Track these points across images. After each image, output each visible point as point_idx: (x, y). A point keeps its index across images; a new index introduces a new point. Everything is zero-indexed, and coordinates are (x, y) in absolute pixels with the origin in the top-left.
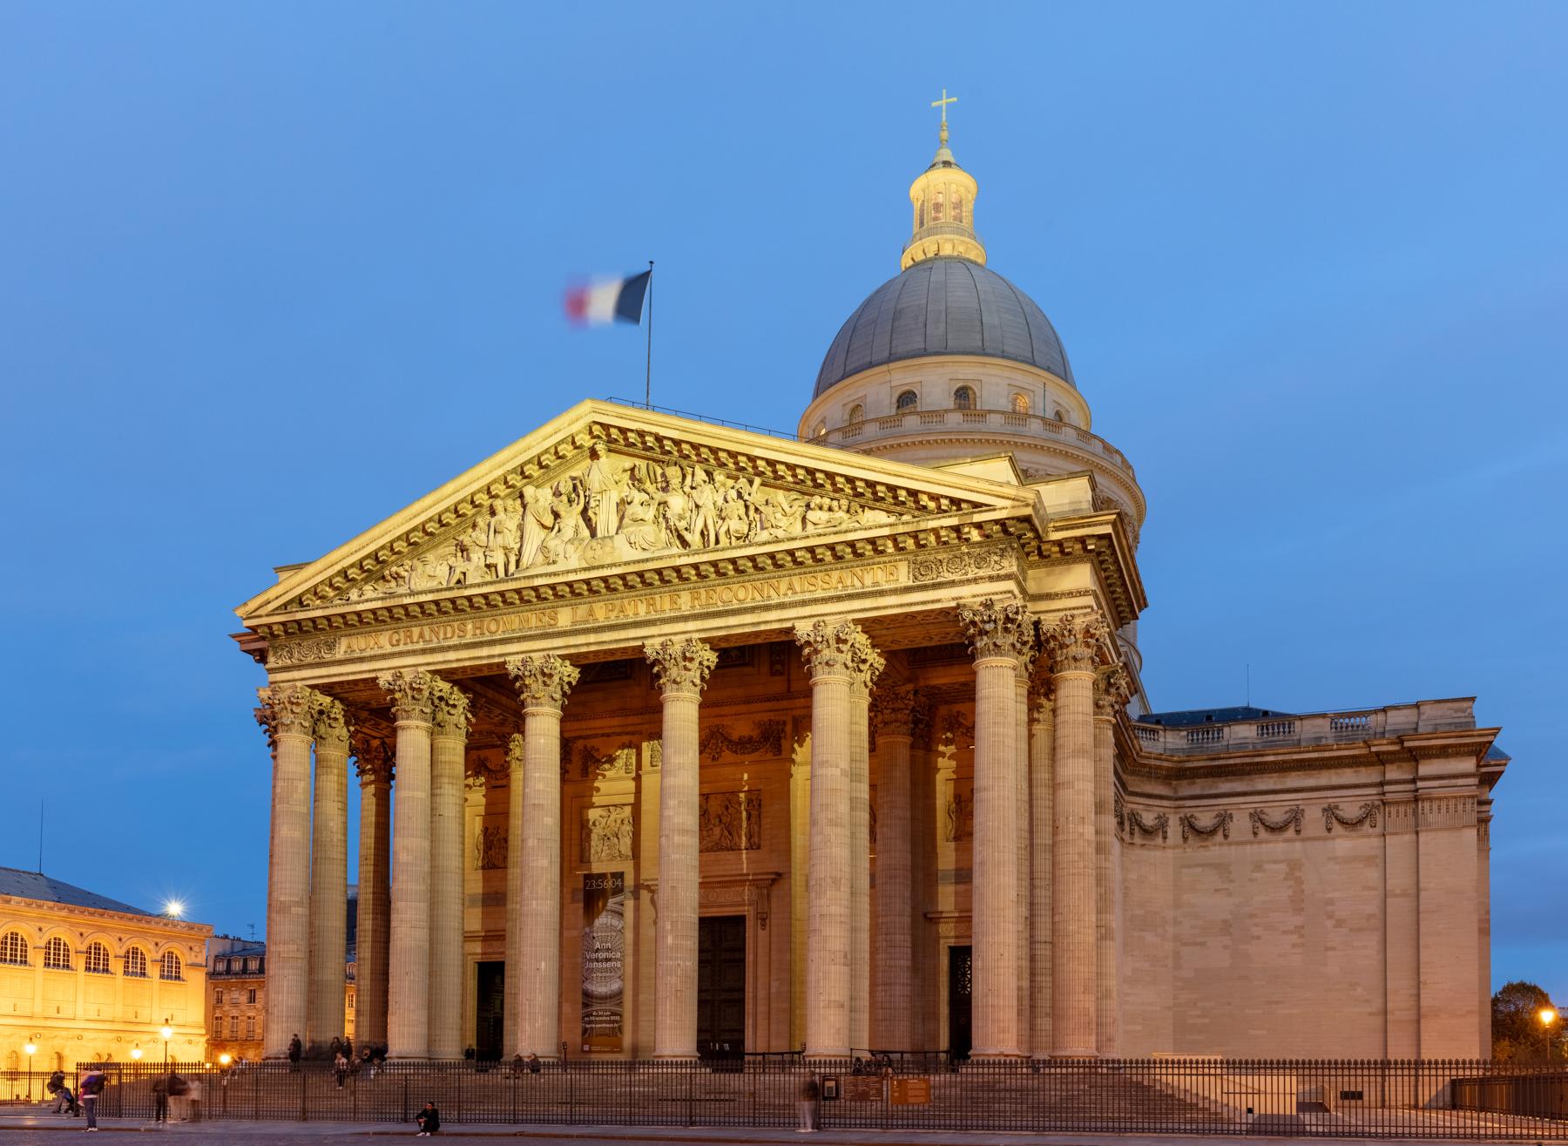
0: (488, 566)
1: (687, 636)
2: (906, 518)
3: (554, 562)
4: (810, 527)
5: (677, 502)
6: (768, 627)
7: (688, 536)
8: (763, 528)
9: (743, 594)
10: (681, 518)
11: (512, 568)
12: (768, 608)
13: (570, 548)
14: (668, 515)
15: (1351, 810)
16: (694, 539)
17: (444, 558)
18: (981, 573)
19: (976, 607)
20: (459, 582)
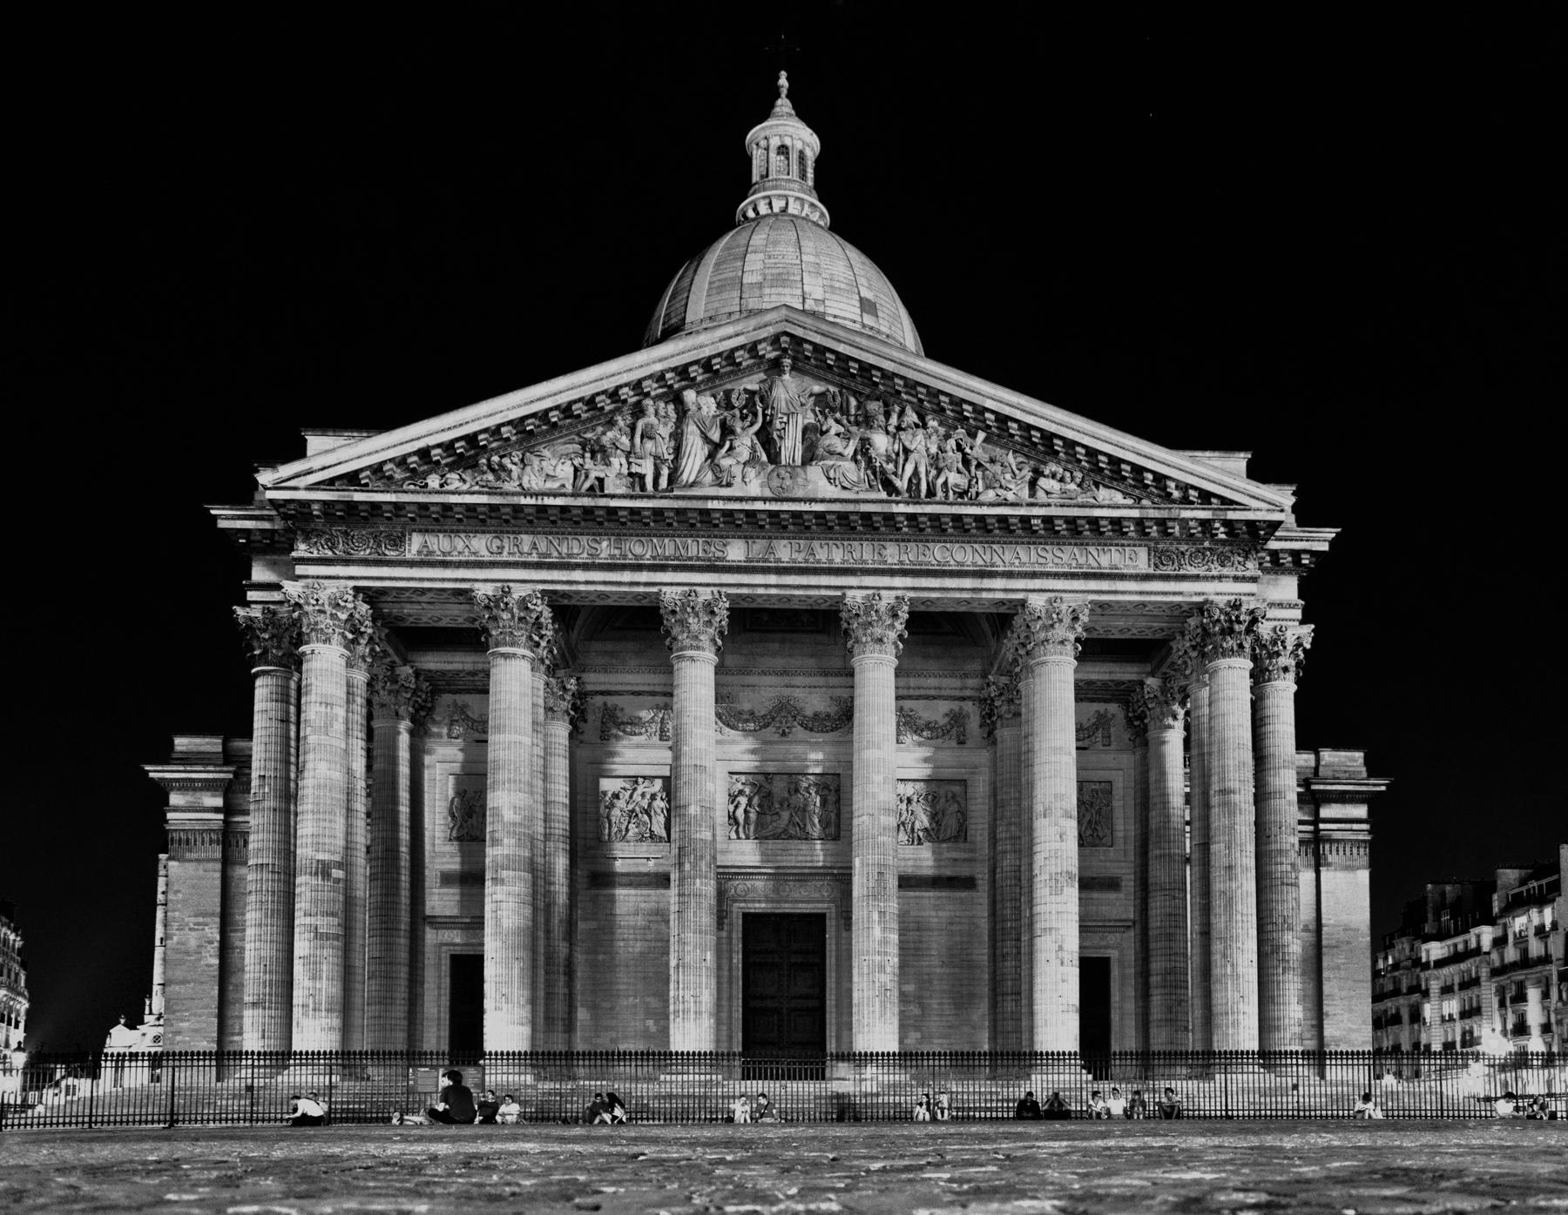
0: (630, 474)
1: (900, 593)
2: (1145, 502)
3: (729, 485)
4: (1041, 495)
5: (881, 443)
6: (990, 595)
7: (898, 483)
8: (987, 487)
10: (889, 460)
11: (663, 483)
12: (992, 575)
13: (751, 473)
14: (873, 453)
16: (902, 484)
18: (1225, 571)
19: (1222, 605)
20: (591, 488)
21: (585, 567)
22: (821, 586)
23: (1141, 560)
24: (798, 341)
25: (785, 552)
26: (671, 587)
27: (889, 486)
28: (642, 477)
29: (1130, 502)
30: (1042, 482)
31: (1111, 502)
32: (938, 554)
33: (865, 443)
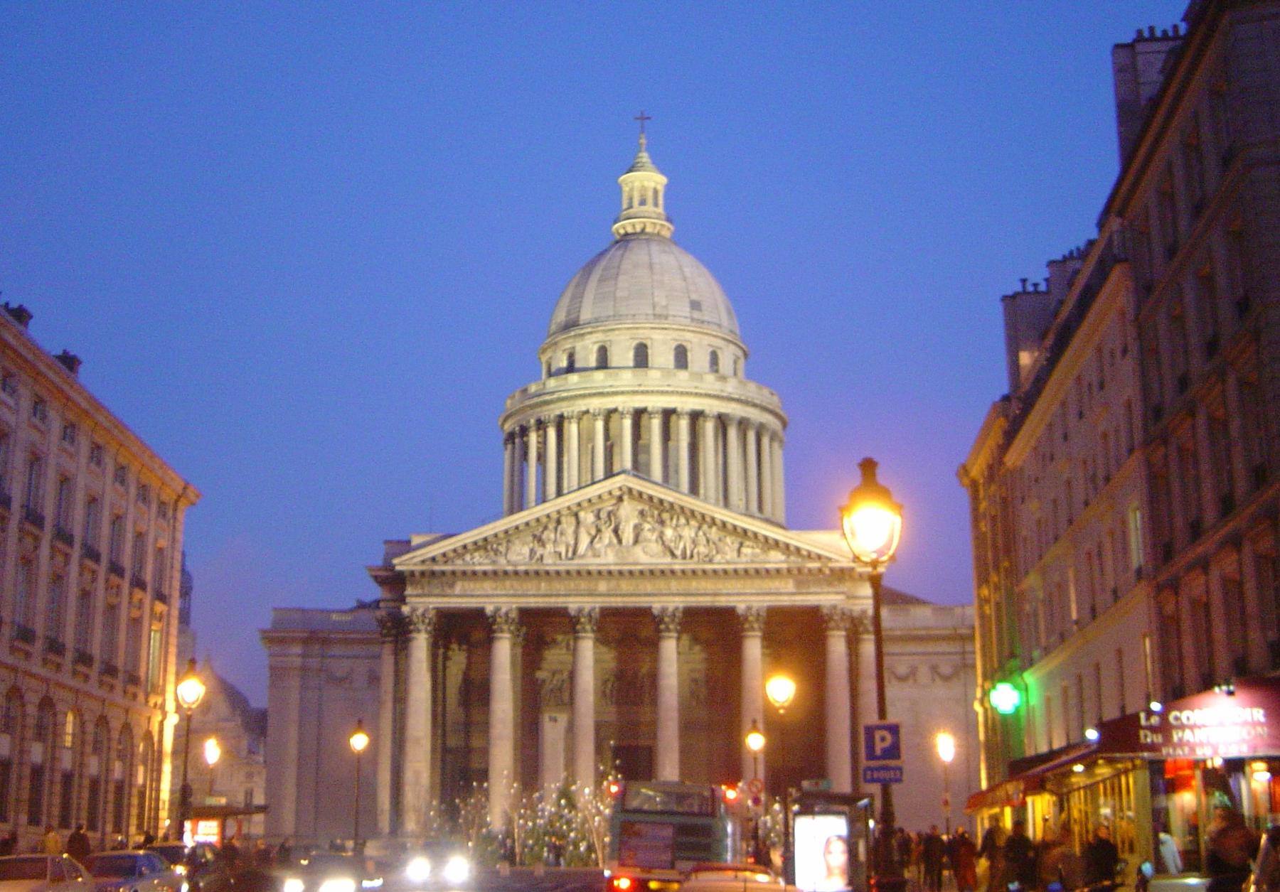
5: (669, 533)
8: (718, 552)
9: (708, 585)
15: (946, 669)
16: (678, 553)
17: (524, 544)
21: (535, 596)
22: (642, 602)
23: (790, 586)
24: (630, 490)
25: (625, 586)
26: (573, 604)
27: (673, 555)
28: (560, 554)
29: (783, 558)
30: (744, 550)
31: (776, 559)
32: (694, 585)
33: (661, 535)
